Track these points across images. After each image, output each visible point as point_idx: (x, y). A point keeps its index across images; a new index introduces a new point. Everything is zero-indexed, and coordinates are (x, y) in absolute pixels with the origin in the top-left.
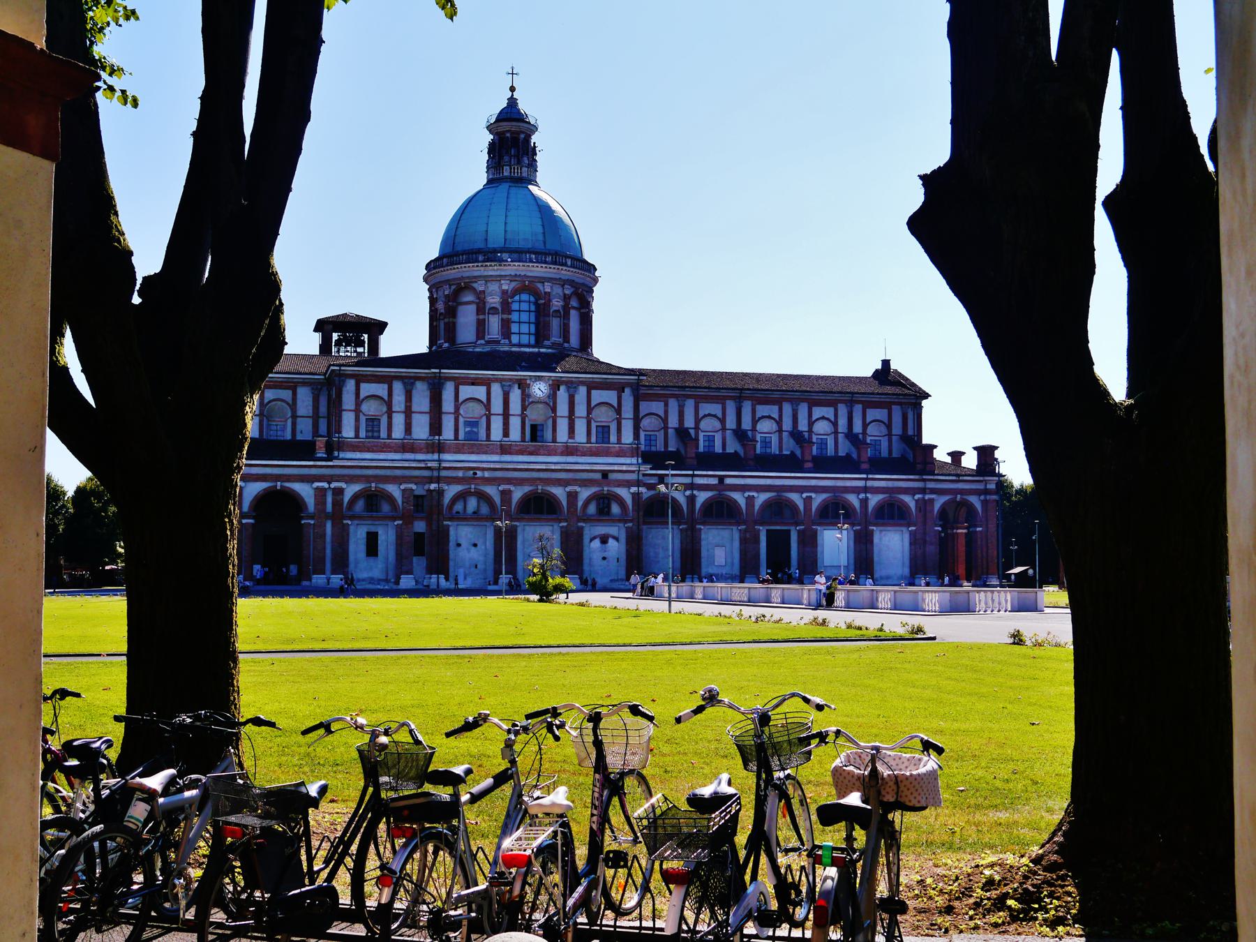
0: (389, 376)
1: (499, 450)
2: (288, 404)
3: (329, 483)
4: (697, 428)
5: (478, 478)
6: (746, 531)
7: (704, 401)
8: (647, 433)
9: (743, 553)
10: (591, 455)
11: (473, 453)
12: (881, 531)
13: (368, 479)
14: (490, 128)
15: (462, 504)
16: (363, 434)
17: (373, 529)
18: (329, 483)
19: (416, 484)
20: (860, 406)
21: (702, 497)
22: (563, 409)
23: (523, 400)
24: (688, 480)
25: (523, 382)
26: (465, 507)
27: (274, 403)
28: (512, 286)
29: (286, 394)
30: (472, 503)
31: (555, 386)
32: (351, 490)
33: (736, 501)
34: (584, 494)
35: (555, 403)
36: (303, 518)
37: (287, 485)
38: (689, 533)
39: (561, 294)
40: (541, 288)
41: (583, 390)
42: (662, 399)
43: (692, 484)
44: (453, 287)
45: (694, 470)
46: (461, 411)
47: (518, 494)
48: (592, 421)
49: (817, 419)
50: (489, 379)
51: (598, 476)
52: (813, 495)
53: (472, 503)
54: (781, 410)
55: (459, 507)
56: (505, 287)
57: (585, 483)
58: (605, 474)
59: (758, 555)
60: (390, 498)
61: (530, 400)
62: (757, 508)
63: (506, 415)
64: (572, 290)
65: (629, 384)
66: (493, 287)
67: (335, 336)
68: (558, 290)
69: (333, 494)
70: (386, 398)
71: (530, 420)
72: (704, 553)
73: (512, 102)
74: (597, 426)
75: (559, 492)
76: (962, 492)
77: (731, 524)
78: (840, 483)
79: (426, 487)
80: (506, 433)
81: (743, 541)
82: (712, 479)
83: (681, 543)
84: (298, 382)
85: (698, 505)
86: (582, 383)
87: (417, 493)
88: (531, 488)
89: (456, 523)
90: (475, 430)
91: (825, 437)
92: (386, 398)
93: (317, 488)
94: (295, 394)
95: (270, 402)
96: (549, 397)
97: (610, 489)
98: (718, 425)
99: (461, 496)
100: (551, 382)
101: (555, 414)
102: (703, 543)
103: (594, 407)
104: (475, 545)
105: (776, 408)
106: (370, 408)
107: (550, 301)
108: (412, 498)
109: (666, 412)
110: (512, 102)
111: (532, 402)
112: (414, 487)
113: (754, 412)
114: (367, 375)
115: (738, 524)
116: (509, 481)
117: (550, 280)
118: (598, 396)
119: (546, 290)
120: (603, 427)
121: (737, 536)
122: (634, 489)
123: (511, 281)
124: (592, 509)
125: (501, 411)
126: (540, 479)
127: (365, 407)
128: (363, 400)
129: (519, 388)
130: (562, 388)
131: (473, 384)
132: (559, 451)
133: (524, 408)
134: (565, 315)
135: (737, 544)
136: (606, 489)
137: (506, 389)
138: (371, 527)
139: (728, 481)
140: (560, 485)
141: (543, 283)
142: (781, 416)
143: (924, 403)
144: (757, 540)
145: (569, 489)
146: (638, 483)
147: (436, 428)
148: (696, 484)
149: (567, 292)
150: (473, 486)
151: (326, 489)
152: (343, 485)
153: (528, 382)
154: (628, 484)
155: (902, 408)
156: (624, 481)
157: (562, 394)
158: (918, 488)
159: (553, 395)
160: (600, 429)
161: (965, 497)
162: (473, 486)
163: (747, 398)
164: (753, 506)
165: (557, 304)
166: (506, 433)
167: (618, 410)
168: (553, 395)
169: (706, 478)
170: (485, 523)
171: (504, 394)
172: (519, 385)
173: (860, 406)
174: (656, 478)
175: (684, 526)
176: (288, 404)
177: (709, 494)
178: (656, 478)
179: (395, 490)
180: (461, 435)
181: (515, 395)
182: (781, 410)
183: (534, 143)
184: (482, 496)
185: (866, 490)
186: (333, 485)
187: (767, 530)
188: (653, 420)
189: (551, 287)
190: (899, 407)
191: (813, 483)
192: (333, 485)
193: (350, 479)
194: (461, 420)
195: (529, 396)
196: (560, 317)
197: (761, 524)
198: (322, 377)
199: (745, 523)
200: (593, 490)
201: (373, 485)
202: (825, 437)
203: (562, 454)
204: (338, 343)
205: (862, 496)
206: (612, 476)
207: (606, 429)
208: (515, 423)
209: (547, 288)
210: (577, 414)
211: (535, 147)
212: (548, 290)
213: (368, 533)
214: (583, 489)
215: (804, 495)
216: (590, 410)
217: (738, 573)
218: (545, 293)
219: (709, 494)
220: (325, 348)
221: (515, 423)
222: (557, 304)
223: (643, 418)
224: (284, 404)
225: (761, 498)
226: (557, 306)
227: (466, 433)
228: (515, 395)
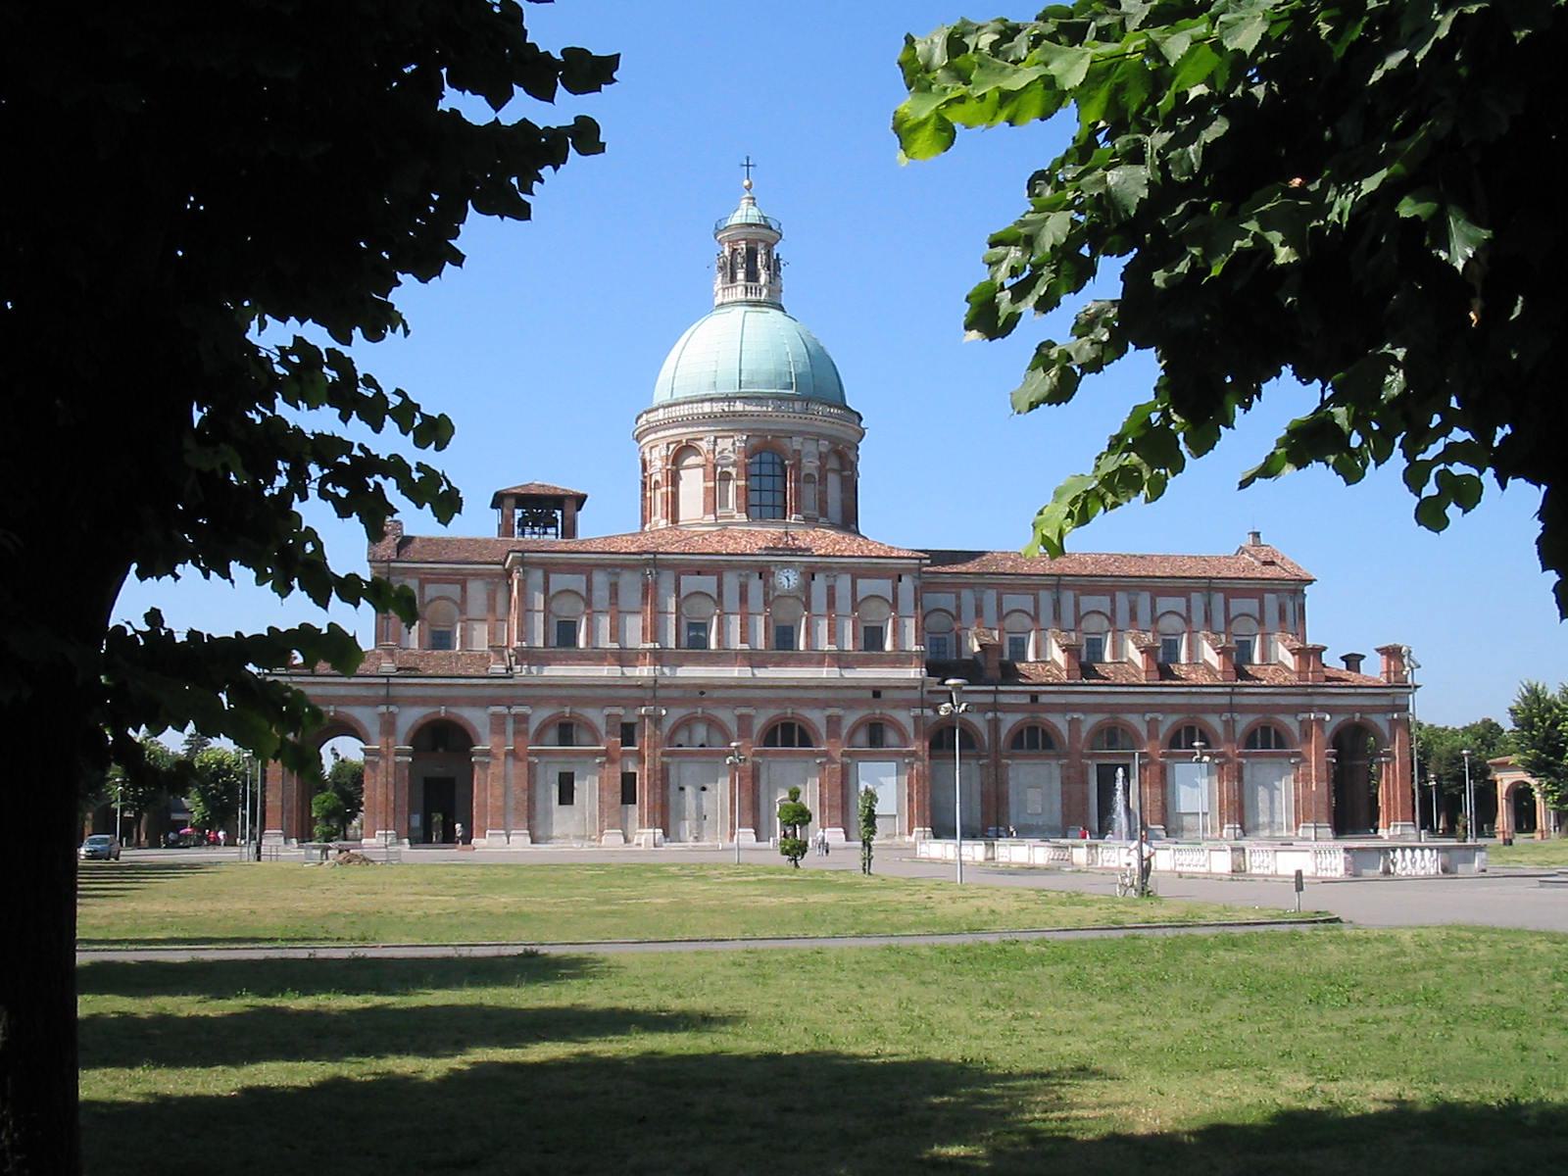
0: (589, 565)
2: (455, 603)
3: (509, 708)
6: (1068, 766)
8: (934, 636)
9: (1066, 796)
12: (1252, 764)
13: (562, 701)
15: (687, 734)
16: (553, 641)
17: (567, 769)
18: (509, 708)
19: (624, 708)
20: (1221, 595)
21: (1009, 721)
23: (766, 594)
24: (989, 699)
26: (690, 737)
27: (438, 602)
29: (454, 591)
30: (701, 732)
31: (810, 574)
32: (539, 716)
33: (1054, 727)
34: (850, 718)
35: (808, 598)
36: (473, 755)
37: (454, 710)
38: (992, 769)
39: (816, 452)
40: (789, 445)
41: (844, 583)
44: (672, 447)
45: (996, 685)
46: (683, 610)
47: (761, 720)
49: (1163, 614)
50: (720, 566)
51: (870, 694)
52: (1160, 717)
53: (701, 732)
54: (1113, 601)
55: (682, 737)
57: (851, 704)
58: (877, 693)
59: (1085, 799)
60: (591, 728)
62: (1084, 735)
65: (908, 571)
67: (518, 513)
68: (811, 447)
69: (515, 722)
70: (584, 593)
72: (1012, 798)
74: (865, 628)
75: (816, 717)
76: (1362, 709)
77: (1048, 757)
78: (1196, 700)
79: (637, 712)
81: (1066, 780)
82: (1022, 696)
83: (982, 784)
84: (473, 575)
85: (1004, 732)
86: (845, 569)
87: (625, 721)
88: (778, 712)
89: (678, 759)
90: (702, 634)
91: (1174, 638)
92: (584, 593)
93: (493, 714)
94: (464, 589)
95: (431, 601)
96: (799, 588)
99: (686, 723)
100: (802, 569)
102: (1011, 783)
104: (704, 789)
105: (1107, 600)
106: (565, 608)
107: (800, 461)
108: (619, 726)
111: (779, 596)
112: (620, 711)
113: (1077, 605)
114: (557, 564)
115: (1059, 757)
116: (747, 703)
117: (801, 433)
118: (866, 586)
119: (796, 447)
121: (1057, 773)
124: (862, 737)
126: (789, 699)
127: (554, 605)
128: (554, 596)
130: (820, 578)
131: (699, 573)
134: (823, 480)
135: (1057, 786)
136: (878, 711)
137: (742, 579)
138: (566, 766)
139: (1043, 699)
140: (817, 707)
142: (1113, 611)
143: (1307, 589)
144: (1084, 781)
145: (830, 711)
146: (923, 704)
148: (1000, 704)
149: (823, 449)
151: (504, 716)
152: (530, 712)
154: (908, 705)
155: (1278, 597)
156: (903, 700)
157: (819, 584)
158: (1302, 706)
161: (1368, 716)
162: (700, 710)
163: (1067, 587)
164: (1079, 731)
165: (810, 465)
170: (717, 759)
172: (760, 575)
173: (1221, 595)
175: (985, 761)
176: (455, 603)
177: (1019, 717)
179: (596, 716)
181: (756, 586)
182: (1113, 601)
183: (778, 255)
184: (712, 723)
185: (1232, 708)
186: (515, 710)
187: (1098, 765)
190: (1272, 596)
191: (1160, 700)
192: (515, 710)
193: (535, 702)
194: (684, 623)
195: (775, 588)
196: (814, 482)
197: (1091, 757)
198: (500, 567)
199: (1066, 755)
201: (567, 710)
202: (1174, 638)
204: (522, 523)
205: (1226, 716)
206: (884, 694)
209: (796, 443)
211: (778, 259)
213: (561, 774)
215: (1148, 717)
217: (1060, 825)
218: (795, 451)
219: (1019, 717)
220: (506, 529)
222: (810, 465)
224: (451, 605)
225: (1090, 721)
226: (810, 468)
227: (689, 639)
228: (756, 586)
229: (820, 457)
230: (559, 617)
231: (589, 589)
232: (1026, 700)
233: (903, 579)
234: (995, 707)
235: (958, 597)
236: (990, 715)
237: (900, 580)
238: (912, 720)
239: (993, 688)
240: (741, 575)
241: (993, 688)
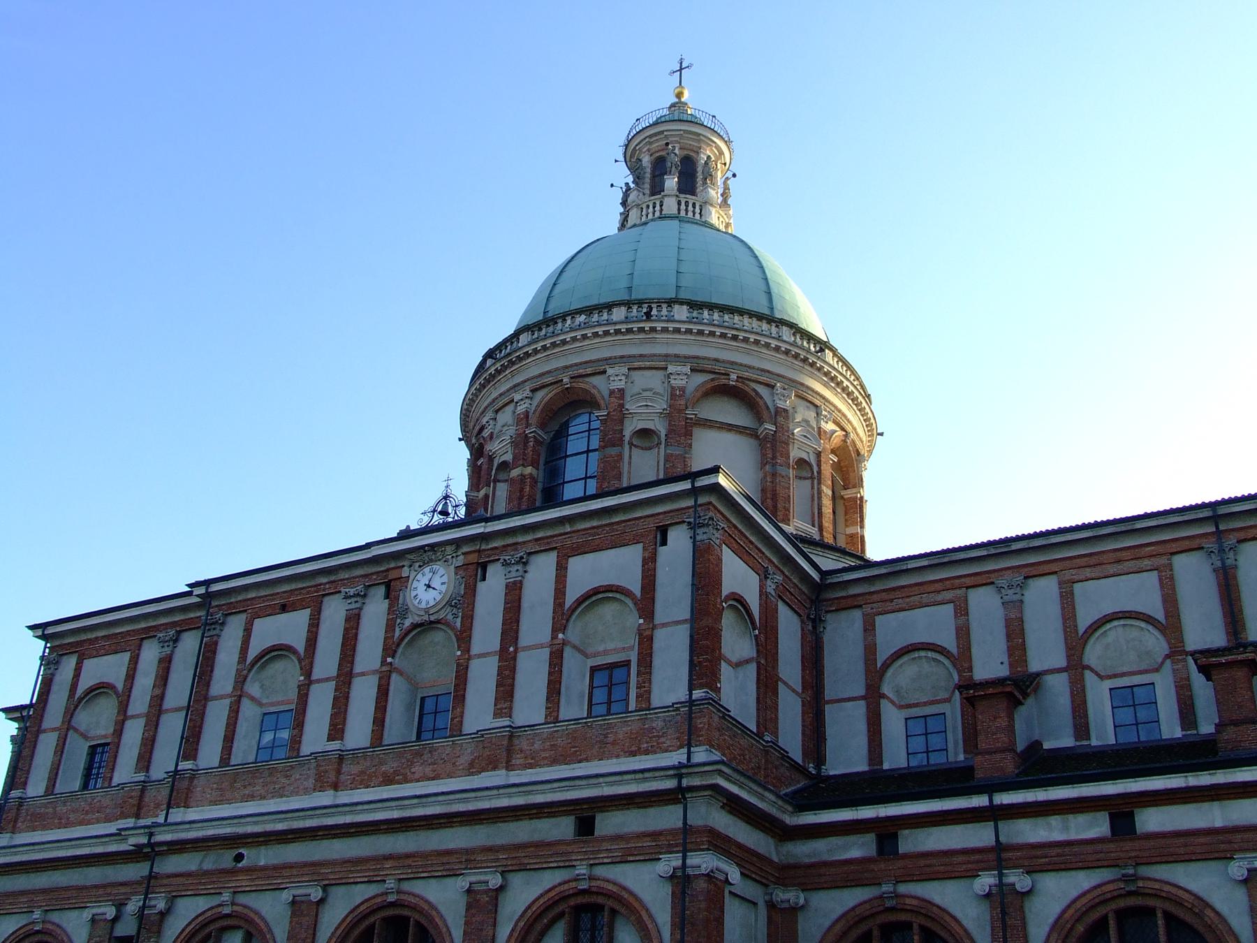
1: (310, 782)
4: (1075, 667)
5: (248, 870)
7: (1088, 572)
10: (554, 762)
11: (251, 797)
14: (631, 158)
16: (71, 781)
22: (487, 634)
23: (390, 627)
24: (979, 836)
25: (392, 575)
28: (535, 402)
35: (469, 619)
42: (948, 595)
43: (999, 848)
46: (253, 688)
48: (568, 652)
51: (563, 828)
56: (521, 408)
61: (407, 623)
63: (345, 677)
64: (700, 379)
66: (506, 417)
68: (653, 380)
71: (410, 680)
73: (678, 105)
74: (594, 670)
80: (337, 731)
88: (372, 890)
97: (600, 871)
98: (1156, 643)
100: (460, 561)
101: (468, 650)
103: (573, 610)
109: (963, 633)
110: (678, 105)
111: (415, 626)
120: (612, 667)
122: (669, 863)
123: (534, 391)
125: (333, 671)
129: (387, 596)
132: (464, 760)
133: (390, 649)
139: (1152, 820)
141: (604, 372)
146: (687, 838)
147: (190, 743)
150: (226, 897)
153: (405, 572)
159: (464, 601)
160: (601, 678)
166: (337, 731)
167: (646, 604)
168: (464, 601)
169: (1055, 821)
171: (348, 620)
172: (388, 585)
174: (870, 838)
177: (1081, 882)
178: (870, 838)
180: (244, 751)
188: (926, 667)
189: (627, 376)
195: (405, 612)
200: (549, 880)
203: (473, 768)
206: (608, 823)
207: (619, 674)
208: (363, 694)
209: (616, 378)
210: (525, 638)
212: (617, 384)
214: (516, 880)
216: (562, 617)
218: (612, 392)
219: (1083, 881)
221: (363, 694)
223: (887, 665)
229: (673, 396)
230: (93, 739)
231: (131, 676)
232: (1095, 827)
233: (672, 534)
234: (998, 857)
235: (962, 610)
236: (986, 881)
237: (664, 543)
238: (666, 890)
239: (980, 801)
240: (346, 597)
241: (980, 801)
